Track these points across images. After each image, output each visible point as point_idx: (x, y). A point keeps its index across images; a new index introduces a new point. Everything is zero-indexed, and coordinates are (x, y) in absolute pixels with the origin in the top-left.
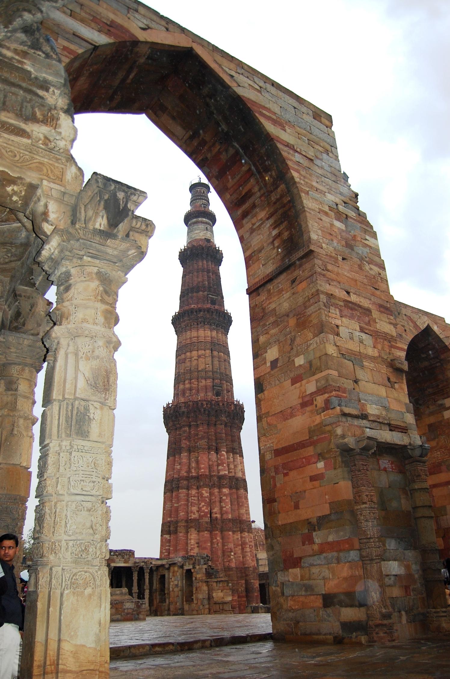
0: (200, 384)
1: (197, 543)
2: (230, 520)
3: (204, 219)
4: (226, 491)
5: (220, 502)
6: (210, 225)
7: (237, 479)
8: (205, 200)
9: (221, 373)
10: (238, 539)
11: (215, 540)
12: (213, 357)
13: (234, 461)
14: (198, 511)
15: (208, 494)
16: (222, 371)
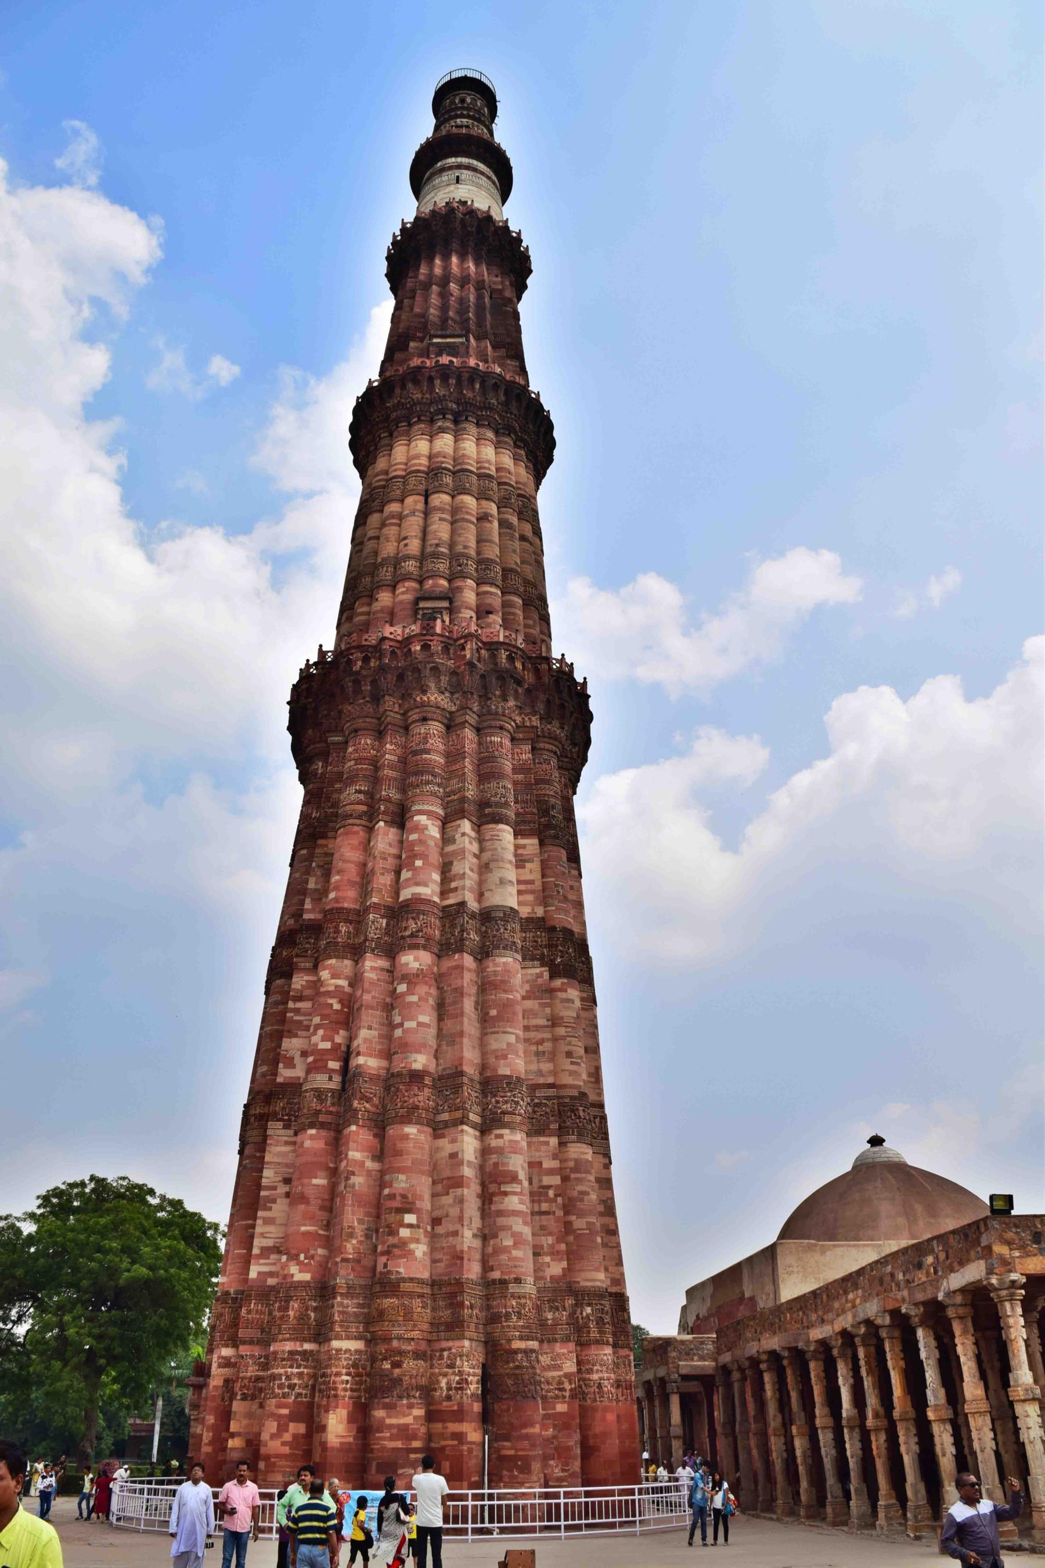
0: (376, 606)
1: (287, 1181)
2: (416, 1077)
3: (453, 160)
4: (413, 960)
5: (389, 1008)
6: (475, 170)
7: (486, 916)
8: (462, 116)
9: (456, 557)
10: (453, 1156)
11: (344, 1164)
12: (427, 513)
13: (482, 850)
14: (304, 1054)
15: (343, 983)
16: (459, 548)
